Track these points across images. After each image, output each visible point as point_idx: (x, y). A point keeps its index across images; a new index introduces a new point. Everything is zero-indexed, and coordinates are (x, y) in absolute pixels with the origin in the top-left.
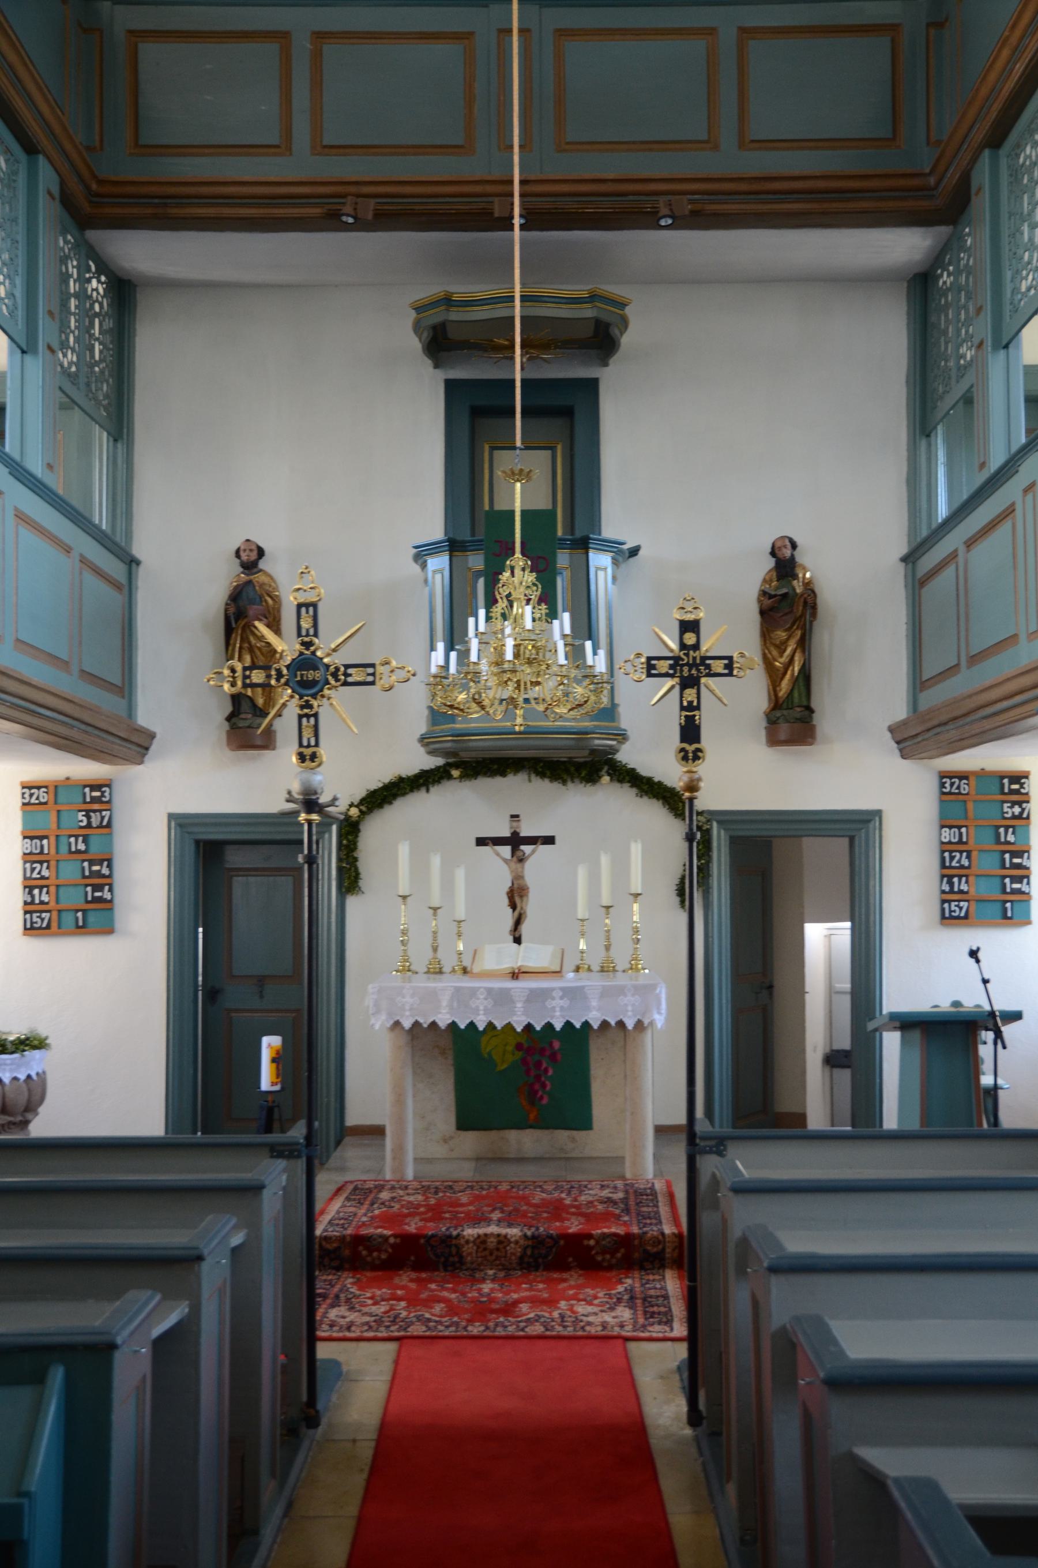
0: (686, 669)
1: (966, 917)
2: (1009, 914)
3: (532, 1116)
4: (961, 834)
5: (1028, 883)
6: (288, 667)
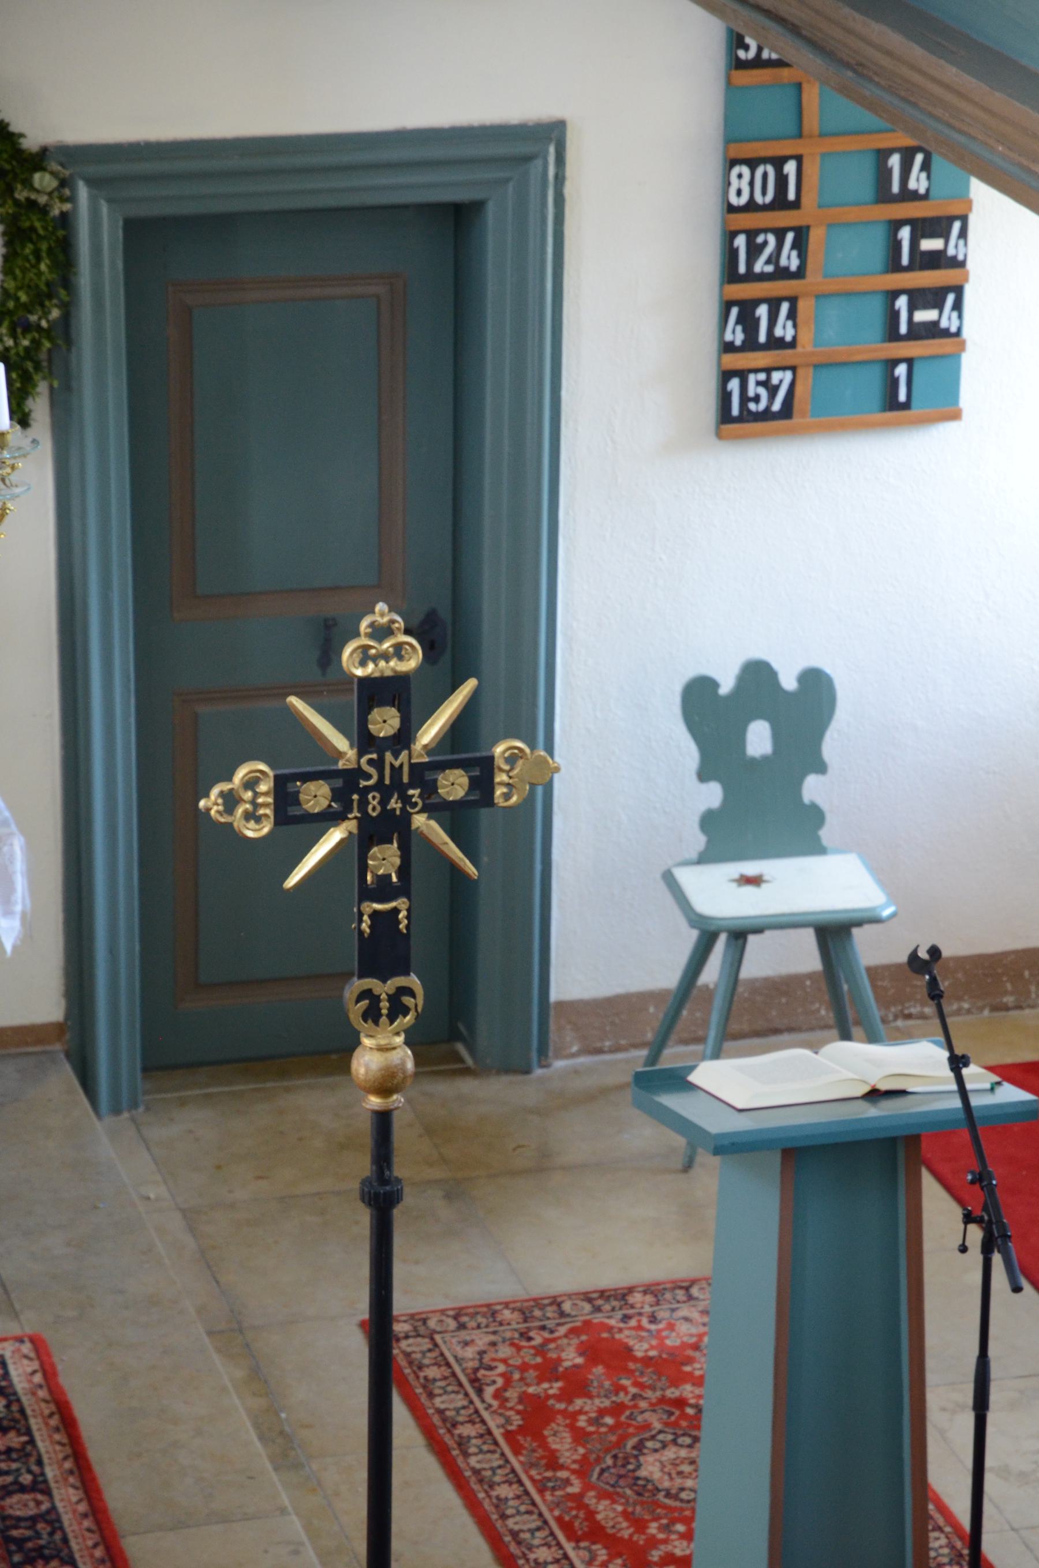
0: (374, 800)
1: (787, 411)
2: (902, 397)
4: (782, 181)
5: (958, 306)
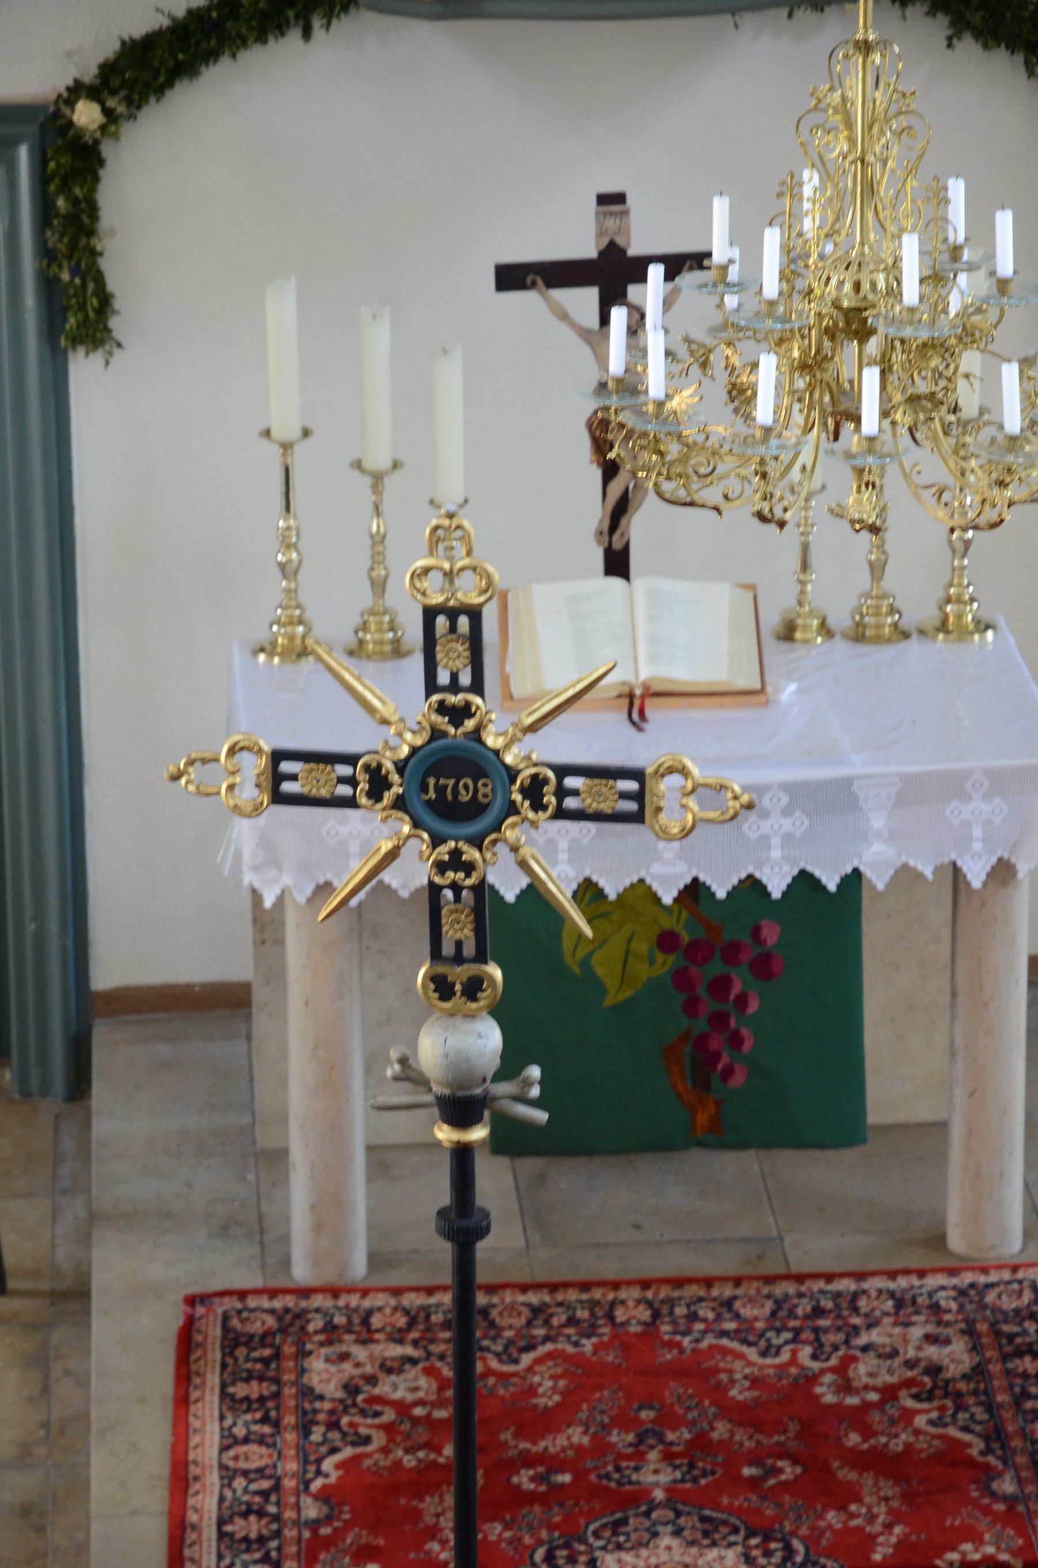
3: (702, 1118)
6: (437, 841)
